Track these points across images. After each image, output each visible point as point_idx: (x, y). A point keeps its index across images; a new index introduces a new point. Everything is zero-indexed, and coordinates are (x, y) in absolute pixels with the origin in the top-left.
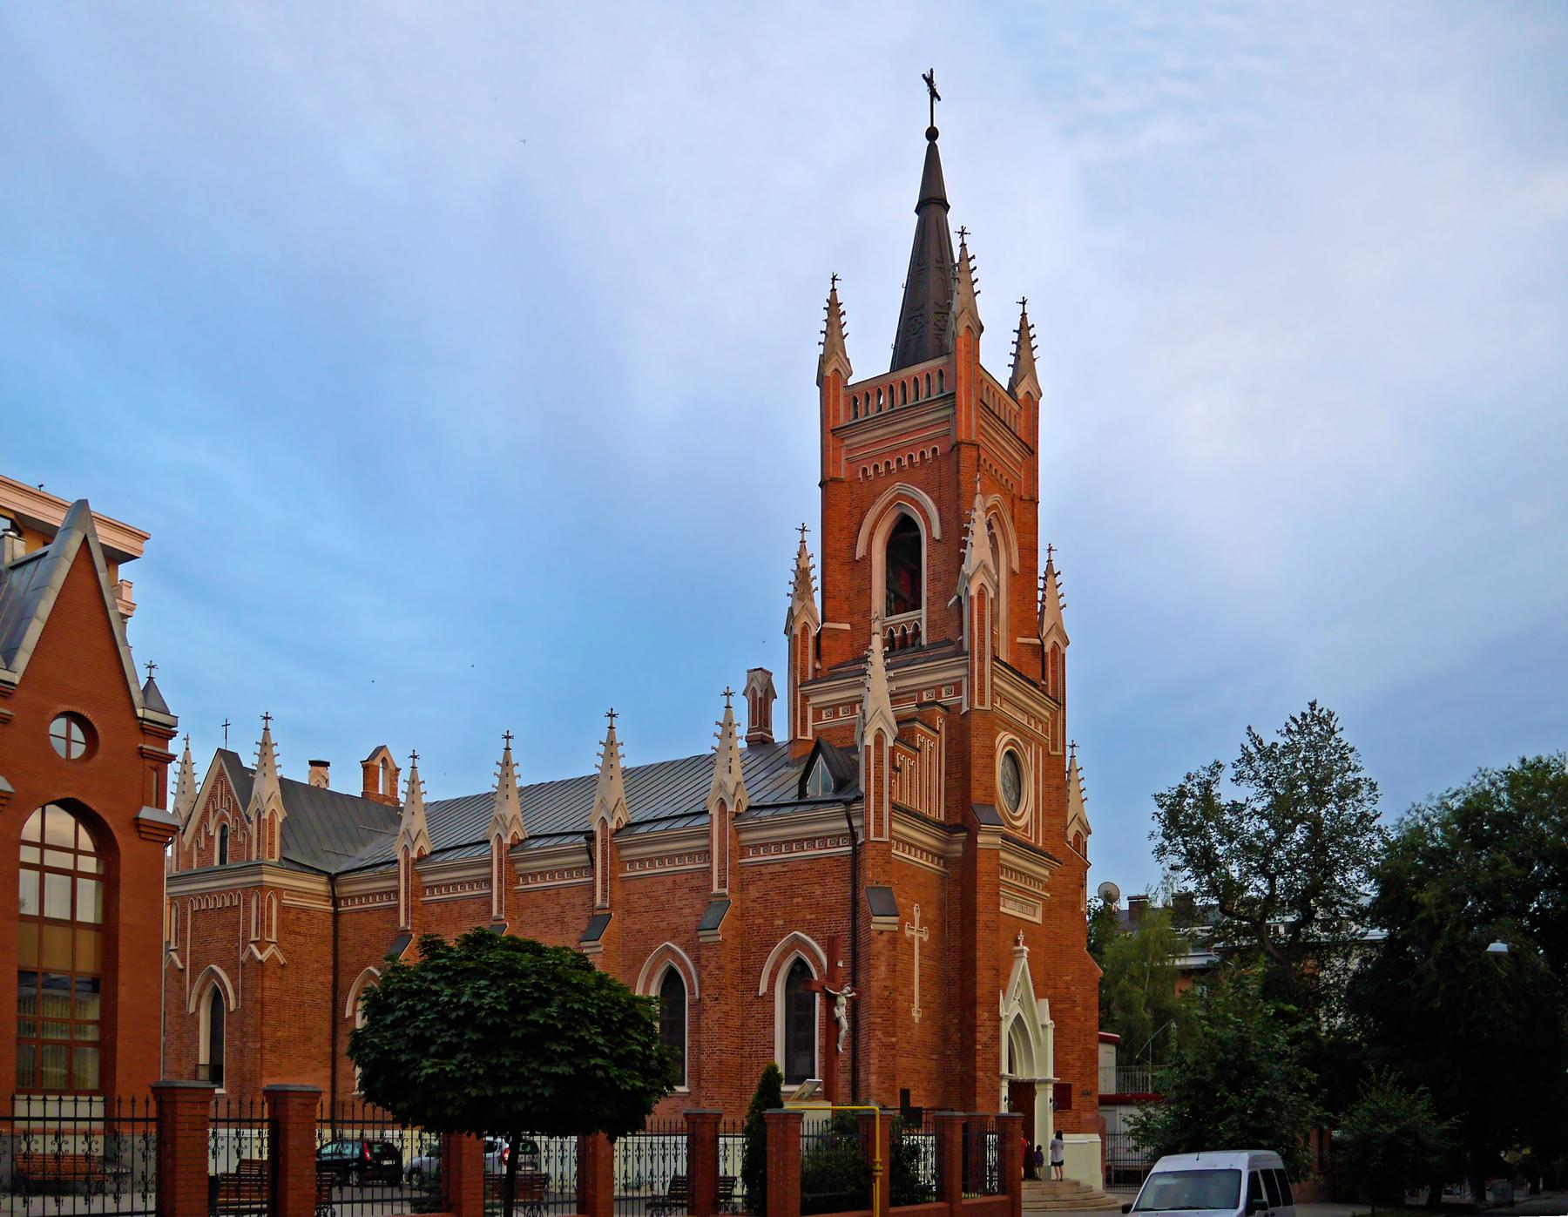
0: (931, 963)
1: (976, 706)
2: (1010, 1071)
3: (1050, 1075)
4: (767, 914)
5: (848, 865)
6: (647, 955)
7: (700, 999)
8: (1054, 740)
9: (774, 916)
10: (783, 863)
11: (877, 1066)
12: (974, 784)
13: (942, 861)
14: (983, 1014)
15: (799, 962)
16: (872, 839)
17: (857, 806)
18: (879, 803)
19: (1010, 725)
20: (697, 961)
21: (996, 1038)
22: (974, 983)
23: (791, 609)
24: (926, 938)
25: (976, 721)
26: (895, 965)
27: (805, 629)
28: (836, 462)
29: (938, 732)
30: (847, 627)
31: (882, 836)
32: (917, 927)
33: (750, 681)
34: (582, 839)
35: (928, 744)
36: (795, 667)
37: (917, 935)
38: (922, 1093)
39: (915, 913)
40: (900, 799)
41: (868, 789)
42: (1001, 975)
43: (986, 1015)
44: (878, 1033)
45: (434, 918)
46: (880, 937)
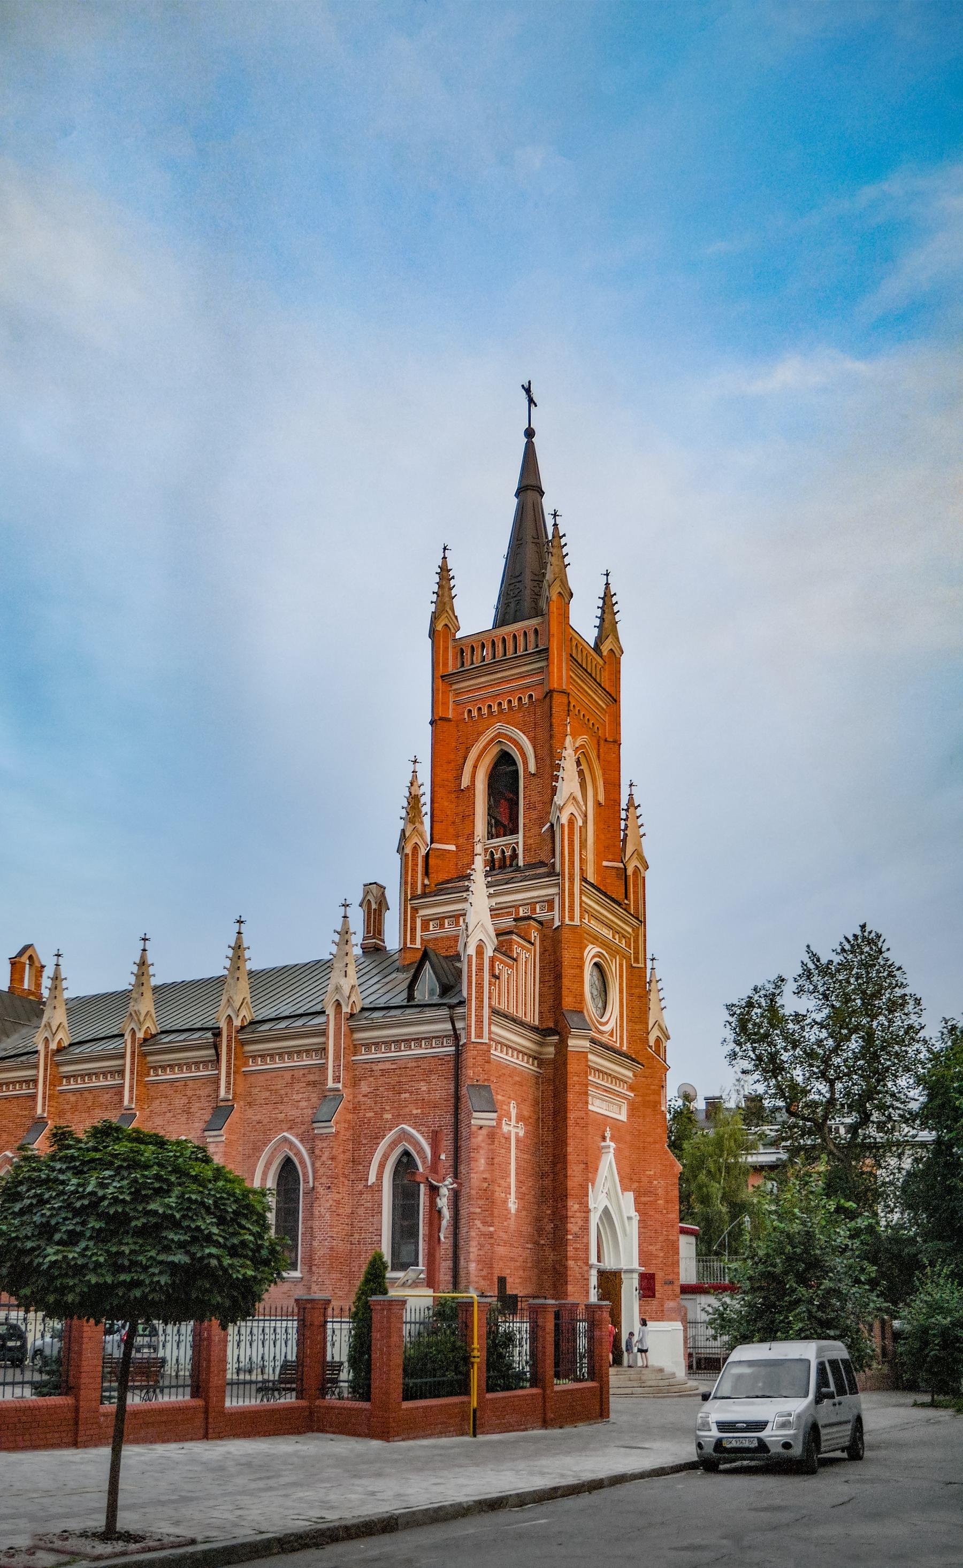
0: (525, 1156)
1: (567, 921)
2: (599, 1261)
3: (635, 1265)
4: (377, 1109)
5: (452, 1065)
6: (265, 1145)
7: (313, 1188)
8: (636, 953)
10: (393, 1060)
11: (476, 1253)
12: (565, 992)
13: (536, 1062)
14: (573, 1206)
15: (406, 1153)
16: (473, 1040)
17: (460, 1010)
18: (480, 1007)
19: (596, 939)
20: (312, 1151)
21: (585, 1229)
22: (566, 1176)
23: (403, 831)
24: (521, 1134)
25: (566, 934)
26: (492, 1159)
27: (416, 848)
28: (445, 704)
29: (533, 944)
30: (453, 848)
31: (482, 1037)
32: (513, 1123)
33: (366, 893)
34: (209, 1034)
35: (523, 956)
36: (406, 883)
37: (513, 1131)
38: (518, 1281)
39: (511, 1110)
40: (499, 1004)
41: (470, 994)
42: (590, 1168)
43: (576, 1207)
44: (478, 1223)
45: (69, 1106)
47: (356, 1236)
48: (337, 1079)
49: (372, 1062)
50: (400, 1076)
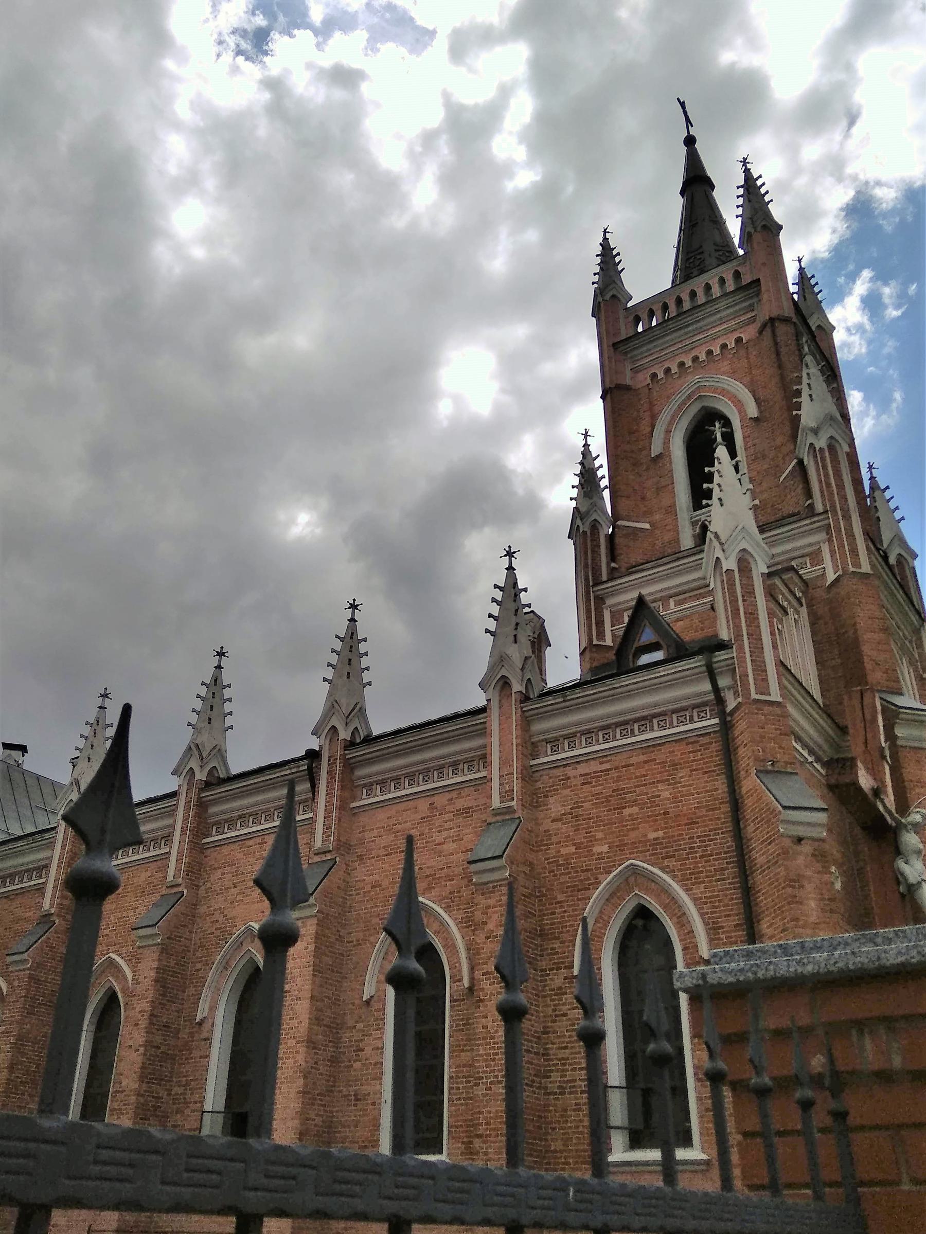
4: (580, 838)
5: (715, 747)
7: (471, 989)
9: (592, 840)
10: (602, 756)
15: (643, 913)
16: (754, 696)
30: (647, 526)
36: (586, 566)
46: (799, 848)
47: (556, 1077)
48: (506, 795)
49: (565, 766)
50: (619, 779)
